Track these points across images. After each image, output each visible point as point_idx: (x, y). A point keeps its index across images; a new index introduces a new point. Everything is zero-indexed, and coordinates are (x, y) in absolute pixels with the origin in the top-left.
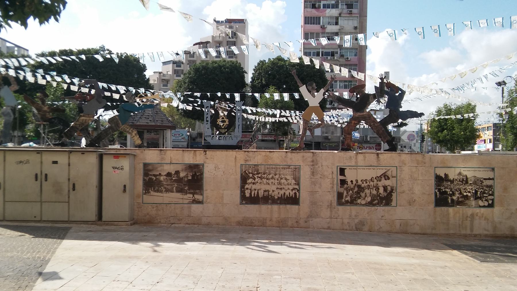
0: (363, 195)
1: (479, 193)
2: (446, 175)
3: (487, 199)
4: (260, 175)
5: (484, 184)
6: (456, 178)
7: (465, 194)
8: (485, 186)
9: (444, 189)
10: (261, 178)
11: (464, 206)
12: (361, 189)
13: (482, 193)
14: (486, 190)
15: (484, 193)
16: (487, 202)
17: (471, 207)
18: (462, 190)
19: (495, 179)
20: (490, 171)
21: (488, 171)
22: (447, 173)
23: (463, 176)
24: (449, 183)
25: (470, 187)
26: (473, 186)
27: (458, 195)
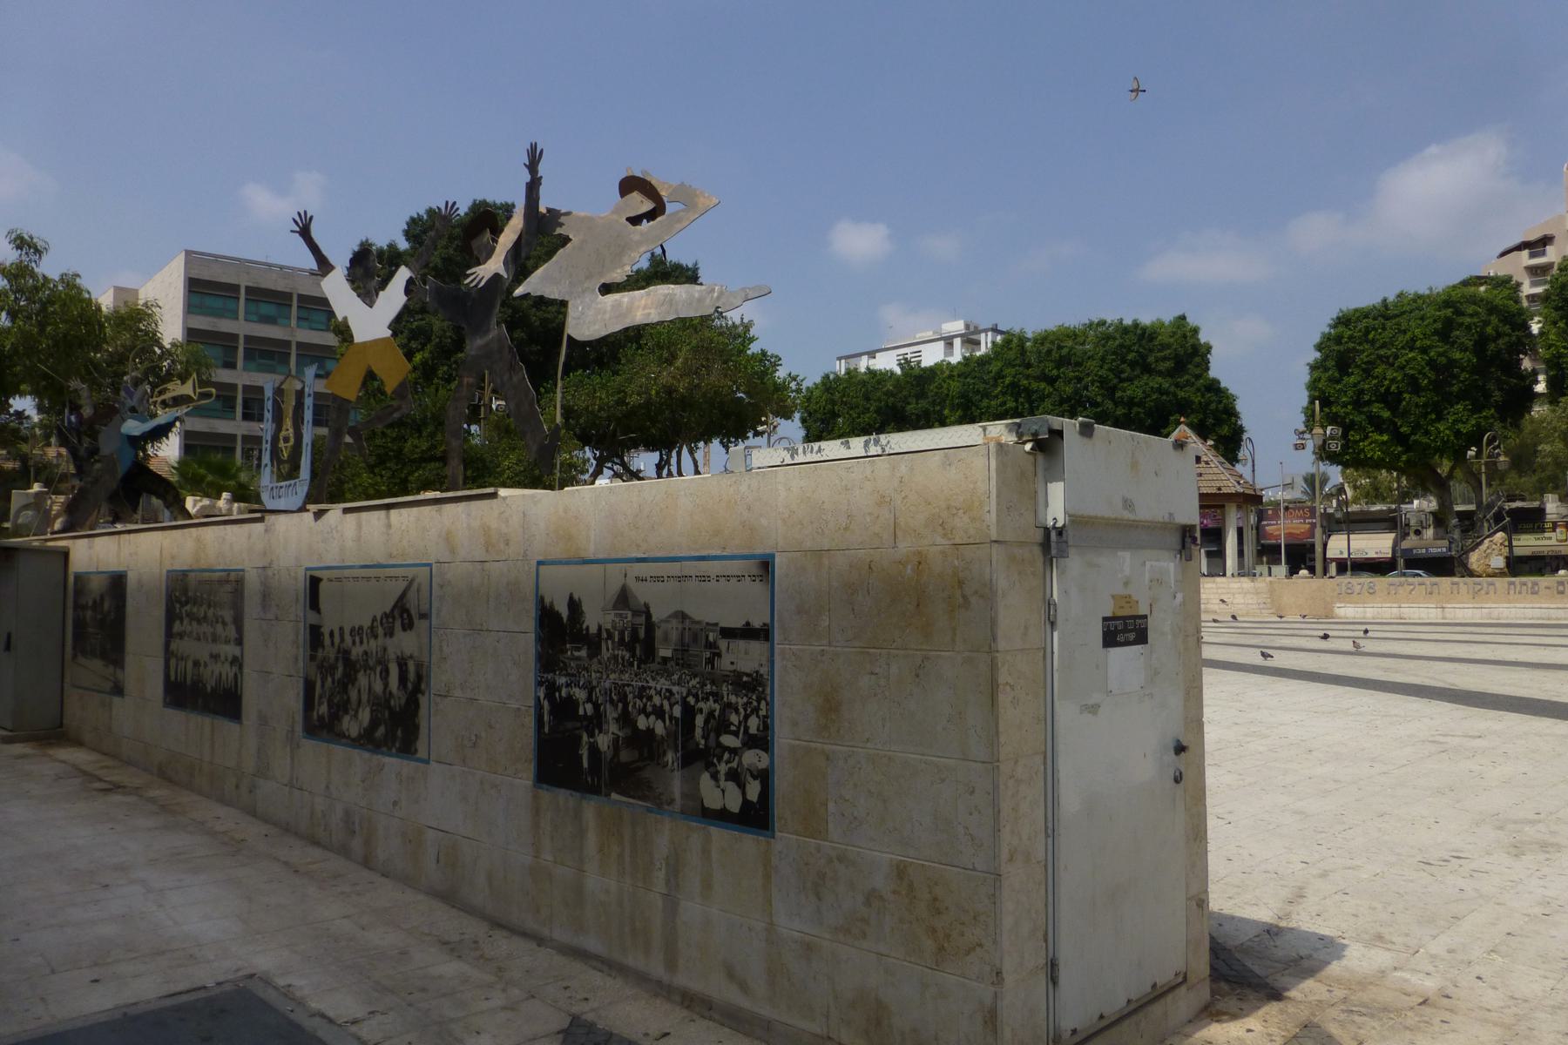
0: (353, 695)
1: (700, 720)
2: (574, 605)
3: (734, 765)
4: (188, 608)
5: (725, 664)
6: (609, 626)
7: (642, 723)
8: (725, 679)
9: (568, 685)
10: (190, 615)
11: (639, 798)
12: (352, 668)
13: (713, 723)
14: (729, 705)
15: (723, 727)
16: (739, 786)
17: (666, 807)
18: (630, 696)
19: (777, 636)
20: (753, 577)
21: (740, 578)
22: (576, 597)
23: (636, 613)
24: (583, 653)
25: (663, 684)
26: (676, 677)
27: (613, 728)
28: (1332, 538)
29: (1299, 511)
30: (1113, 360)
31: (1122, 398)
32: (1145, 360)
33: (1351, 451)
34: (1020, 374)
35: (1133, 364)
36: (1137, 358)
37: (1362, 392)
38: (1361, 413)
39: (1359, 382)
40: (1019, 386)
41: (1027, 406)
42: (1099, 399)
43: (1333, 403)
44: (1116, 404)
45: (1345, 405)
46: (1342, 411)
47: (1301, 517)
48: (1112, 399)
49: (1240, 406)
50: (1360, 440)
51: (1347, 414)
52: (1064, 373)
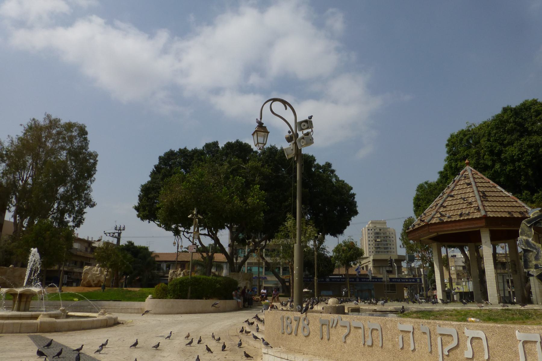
31: (505, 158)
34: (452, 159)
35: (510, 132)
42: (490, 163)
44: (504, 164)
48: (500, 160)
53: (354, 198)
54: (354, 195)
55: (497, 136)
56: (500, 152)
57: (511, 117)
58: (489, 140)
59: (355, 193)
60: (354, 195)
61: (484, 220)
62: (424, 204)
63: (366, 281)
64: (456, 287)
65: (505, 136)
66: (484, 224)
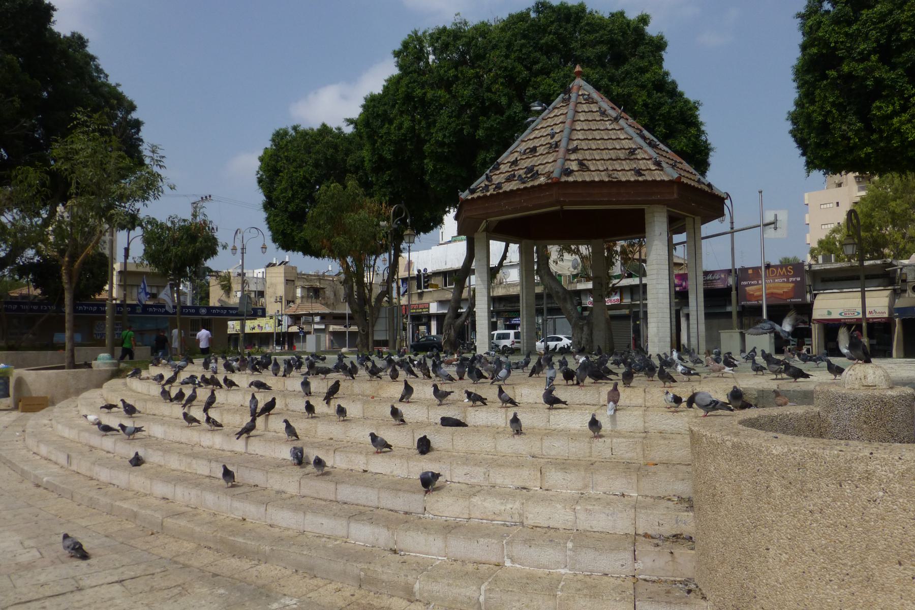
28: (818, 297)
29: (782, 270)
30: (522, 46)
32: (566, 45)
33: (875, 137)
34: (414, 82)
35: (548, 50)
36: (557, 41)
37: (895, 28)
38: (893, 67)
39: (891, 12)
40: (414, 98)
41: (423, 123)
42: (504, 101)
43: (842, 60)
45: (864, 58)
46: (860, 68)
47: (784, 276)
49: (703, 115)
50: (895, 113)
51: (870, 71)
52: (462, 72)
53: (139, 130)
54: (137, 124)
55: (524, 51)
56: (526, 83)
57: (552, 22)
58: (507, 57)
59: (141, 119)
60: (137, 124)
61: (675, 187)
62: (292, 169)
63: (157, 313)
64: (256, 325)
65: (538, 54)
66: (675, 196)
